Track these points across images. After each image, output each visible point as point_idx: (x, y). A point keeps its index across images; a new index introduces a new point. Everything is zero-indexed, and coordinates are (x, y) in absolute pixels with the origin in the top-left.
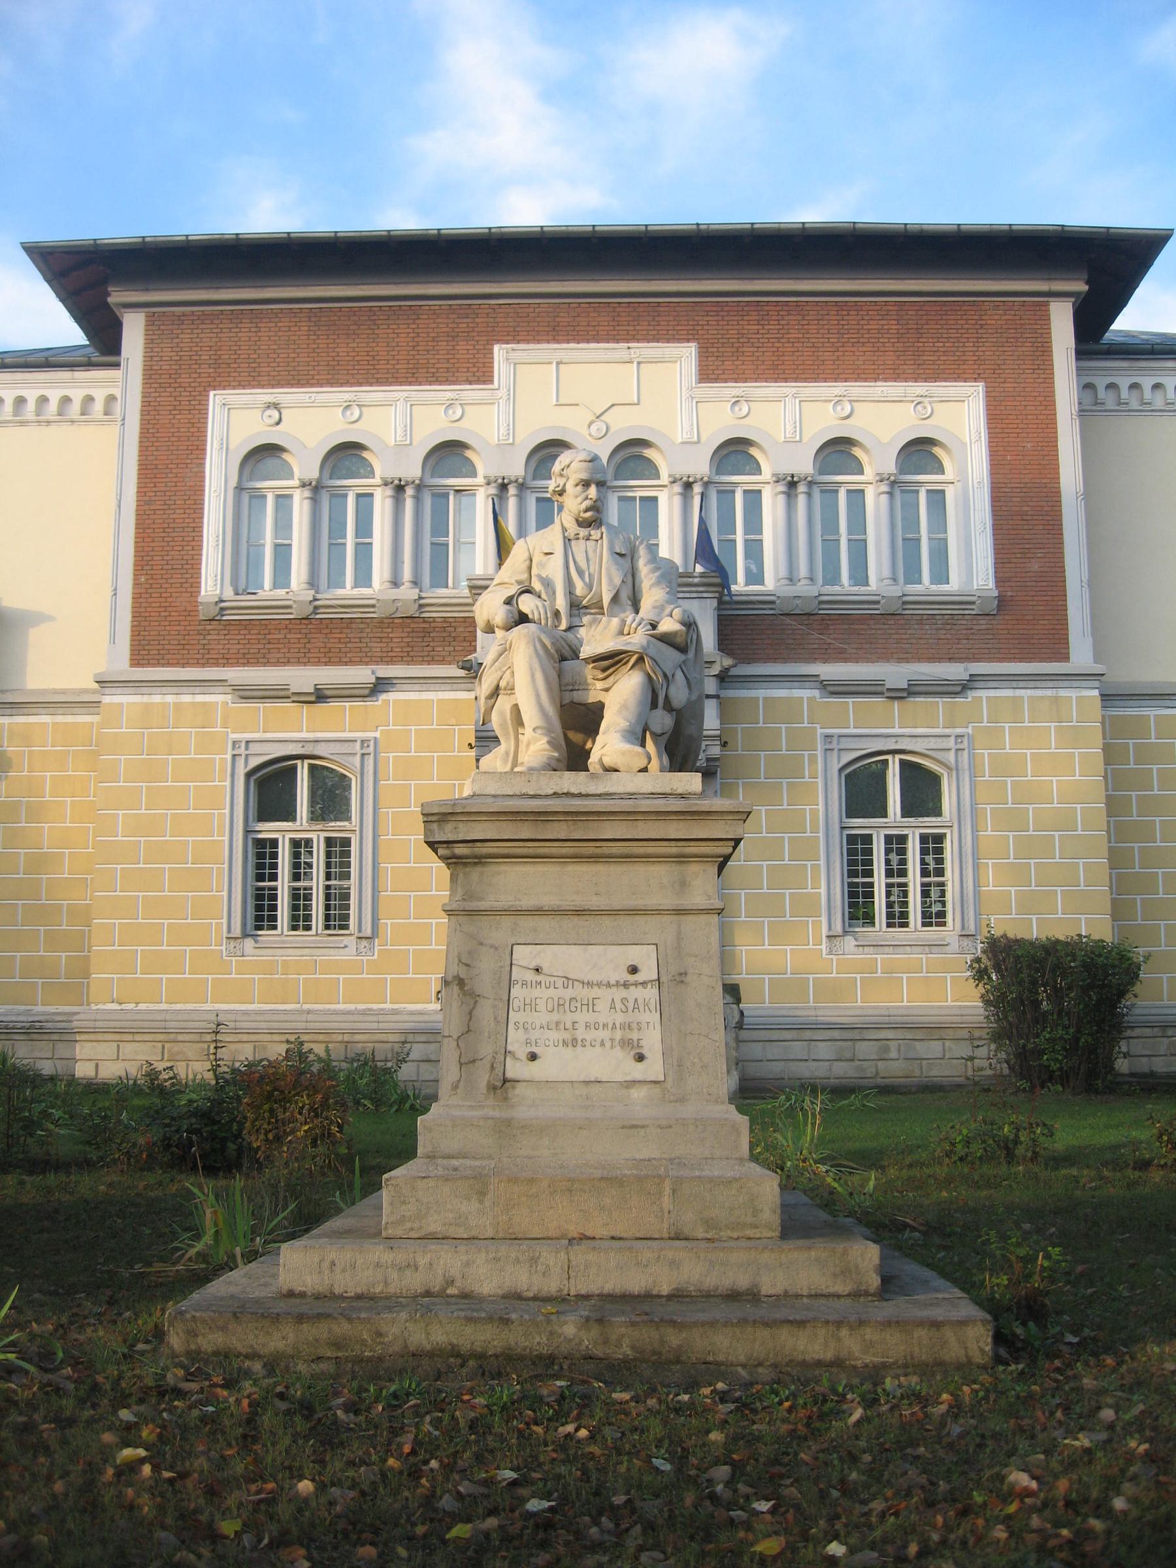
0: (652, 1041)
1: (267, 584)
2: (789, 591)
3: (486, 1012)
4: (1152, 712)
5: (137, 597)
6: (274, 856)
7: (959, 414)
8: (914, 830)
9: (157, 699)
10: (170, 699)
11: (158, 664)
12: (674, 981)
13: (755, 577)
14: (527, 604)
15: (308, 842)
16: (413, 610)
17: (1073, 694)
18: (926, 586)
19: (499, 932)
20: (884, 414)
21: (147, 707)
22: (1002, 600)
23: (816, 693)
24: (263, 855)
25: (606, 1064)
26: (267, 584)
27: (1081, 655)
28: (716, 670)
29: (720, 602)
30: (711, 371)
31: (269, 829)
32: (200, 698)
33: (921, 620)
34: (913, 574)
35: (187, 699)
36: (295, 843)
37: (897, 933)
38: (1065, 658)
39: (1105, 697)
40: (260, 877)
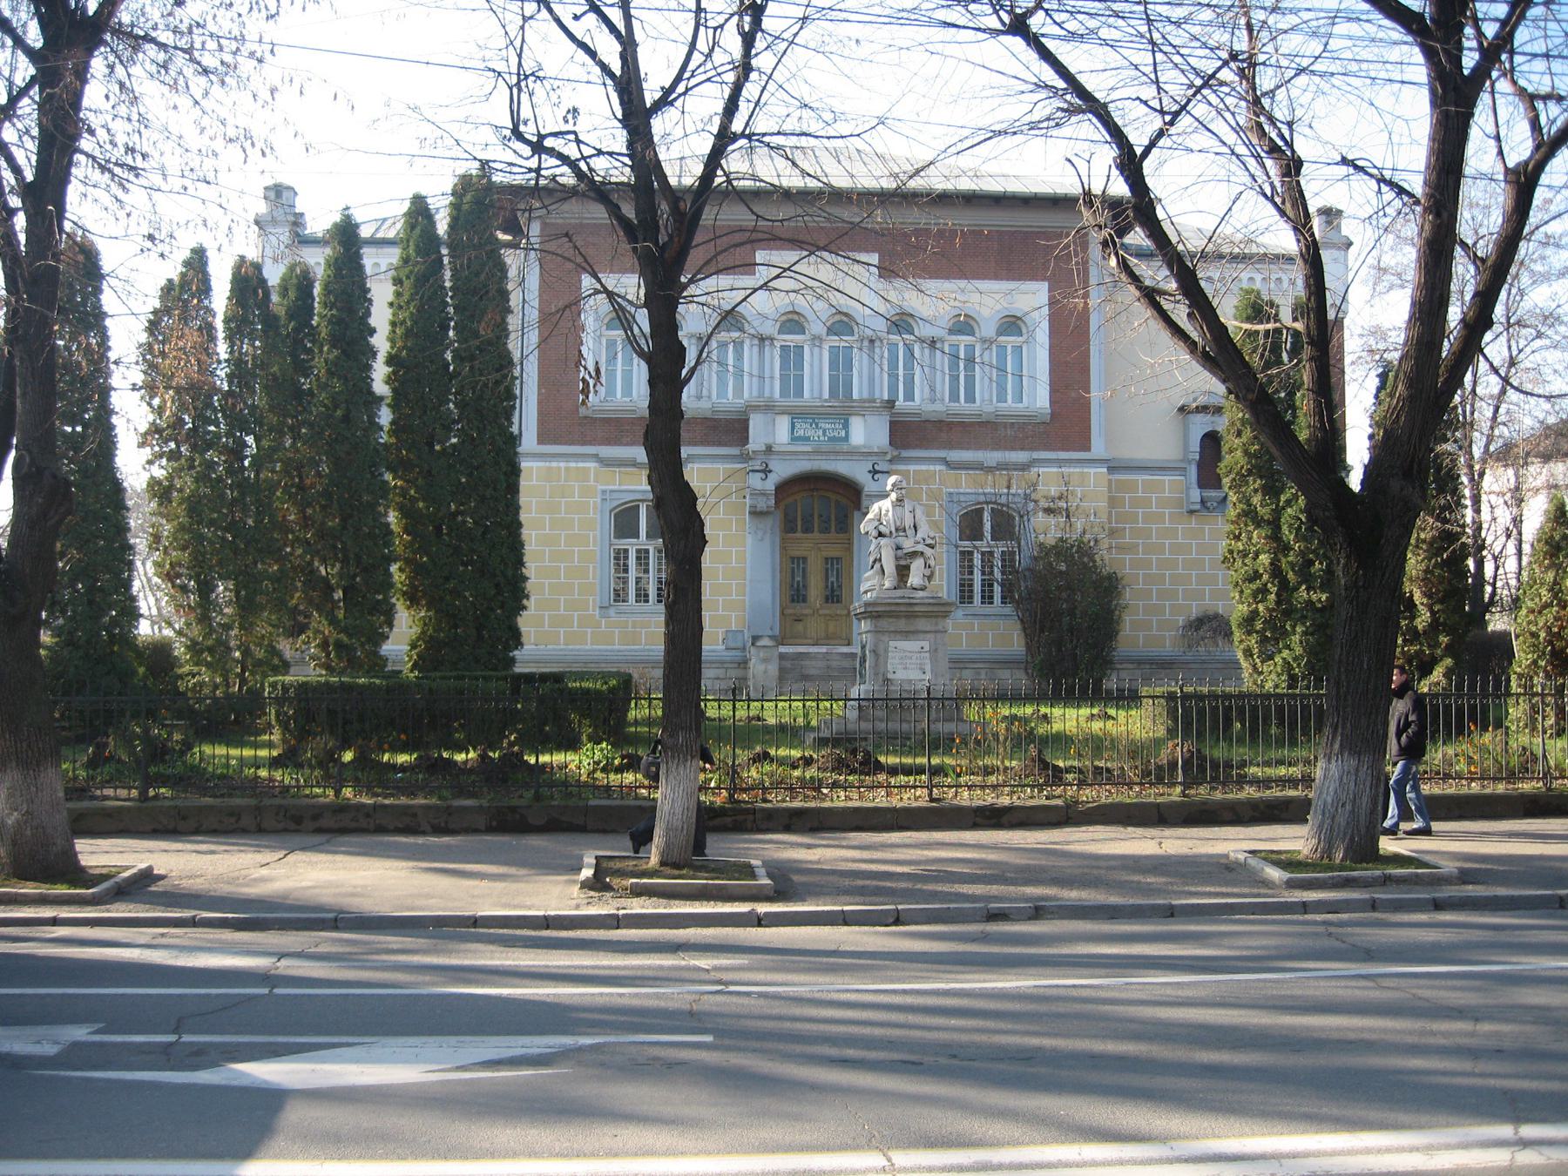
0: (928, 668)
1: (619, 395)
2: (930, 407)
3: (881, 659)
4: (1141, 478)
5: (540, 402)
6: (626, 558)
7: (1032, 298)
8: (999, 548)
9: (554, 464)
10: (562, 465)
11: (555, 443)
12: (934, 651)
13: (909, 396)
14: (882, 529)
15: (647, 551)
16: (709, 415)
17: (1092, 471)
18: (1010, 404)
19: (885, 638)
20: (989, 298)
21: (549, 468)
22: (1053, 414)
23: (943, 468)
24: (620, 557)
25: (914, 675)
26: (619, 395)
27: (1098, 447)
28: (889, 457)
29: (892, 415)
30: (886, 272)
31: (624, 543)
32: (581, 465)
33: (1005, 425)
34: (1002, 397)
35: (573, 465)
36: (638, 551)
37: (988, 609)
38: (1088, 449)
39: (1112, 470)
40: (617, 571)
